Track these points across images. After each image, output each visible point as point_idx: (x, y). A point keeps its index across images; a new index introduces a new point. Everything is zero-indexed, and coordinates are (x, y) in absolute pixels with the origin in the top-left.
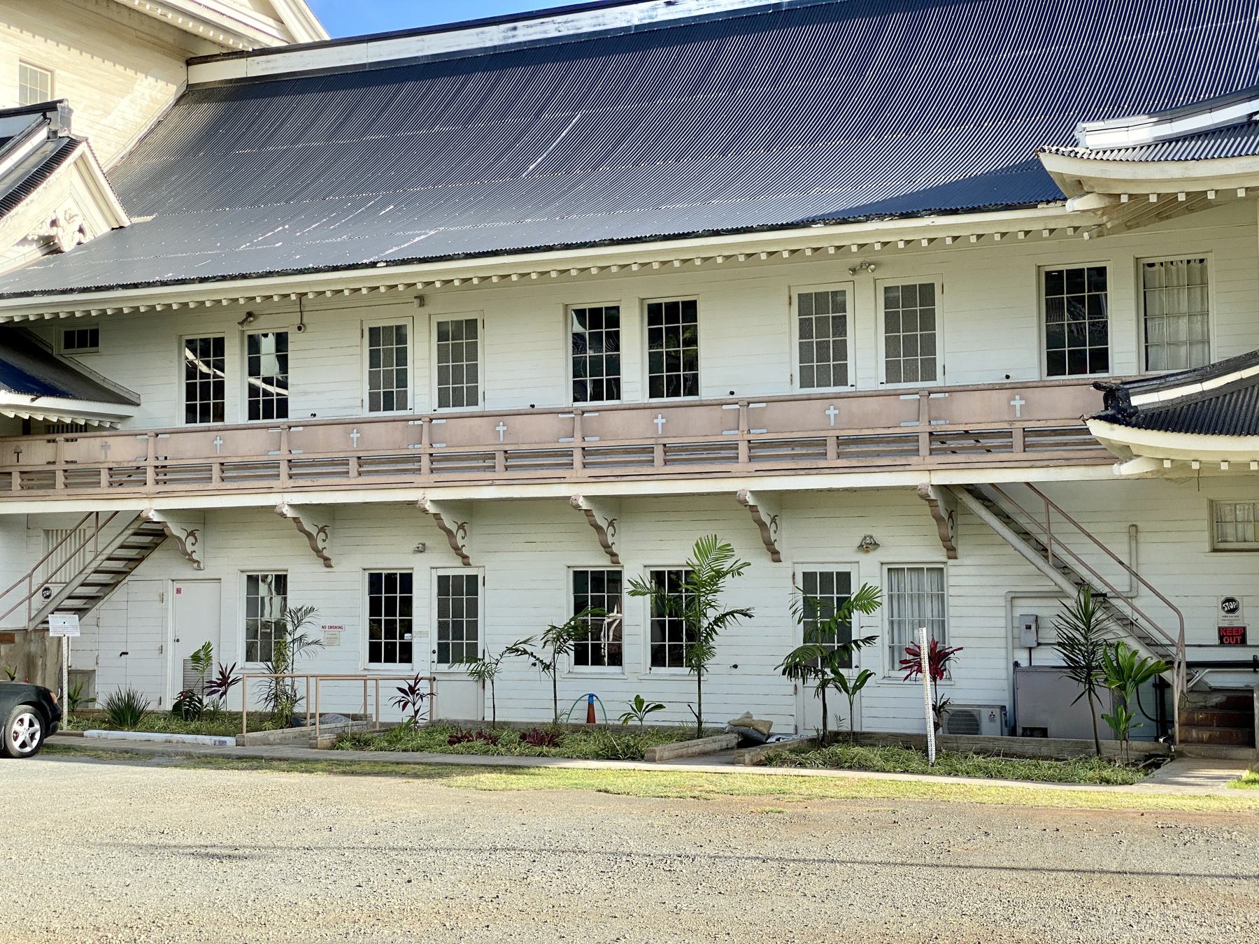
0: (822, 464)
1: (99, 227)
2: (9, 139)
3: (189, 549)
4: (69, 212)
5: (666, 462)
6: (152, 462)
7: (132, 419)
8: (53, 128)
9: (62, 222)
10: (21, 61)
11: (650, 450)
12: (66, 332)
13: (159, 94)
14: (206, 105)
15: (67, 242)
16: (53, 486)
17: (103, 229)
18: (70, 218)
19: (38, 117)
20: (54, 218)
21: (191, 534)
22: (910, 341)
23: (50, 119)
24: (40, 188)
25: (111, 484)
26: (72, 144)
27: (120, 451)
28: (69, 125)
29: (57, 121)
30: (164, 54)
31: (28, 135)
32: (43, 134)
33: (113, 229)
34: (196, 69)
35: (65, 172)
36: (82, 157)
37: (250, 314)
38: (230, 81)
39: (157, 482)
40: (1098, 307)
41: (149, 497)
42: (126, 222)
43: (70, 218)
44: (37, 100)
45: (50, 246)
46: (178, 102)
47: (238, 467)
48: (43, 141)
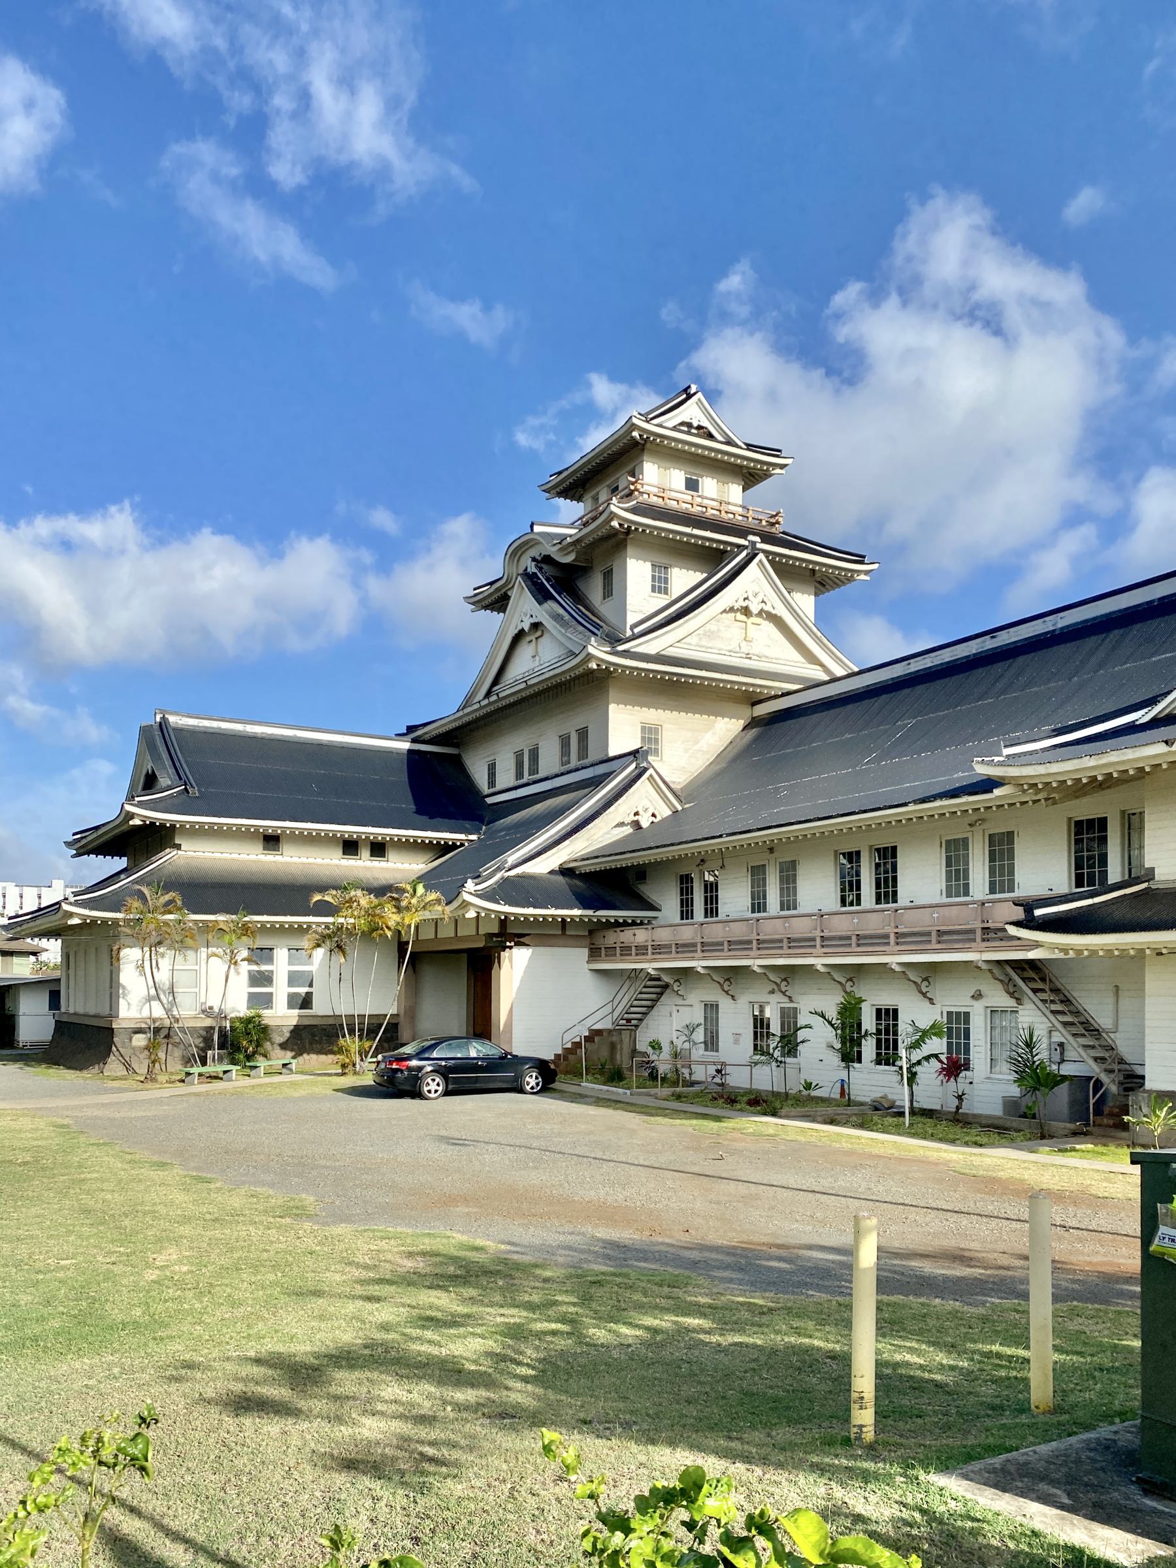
0: (929, 947)
1: (664, 812)
3: (676, 988)
5: (859, 945)
6: (650, 943)
11: (849, 938)
15: (645, 824)
16: (615, 955)
17: (670, 813)
19: (631, 758)
21: (677, 980)
22: (1002, 867)
24: (624, 798)
25: (637, 955)
26: (645, 769)
27: (641, 936)
32: (633, 766)
35: (643, 784)
36: (651, 776)
37: (702, 861)
39: (653, 954)
40: (1103, 840)
41: (650, 961)
42: (680, 808)
45: (637, 825)
46: (744, 729)
47: (684, 945)
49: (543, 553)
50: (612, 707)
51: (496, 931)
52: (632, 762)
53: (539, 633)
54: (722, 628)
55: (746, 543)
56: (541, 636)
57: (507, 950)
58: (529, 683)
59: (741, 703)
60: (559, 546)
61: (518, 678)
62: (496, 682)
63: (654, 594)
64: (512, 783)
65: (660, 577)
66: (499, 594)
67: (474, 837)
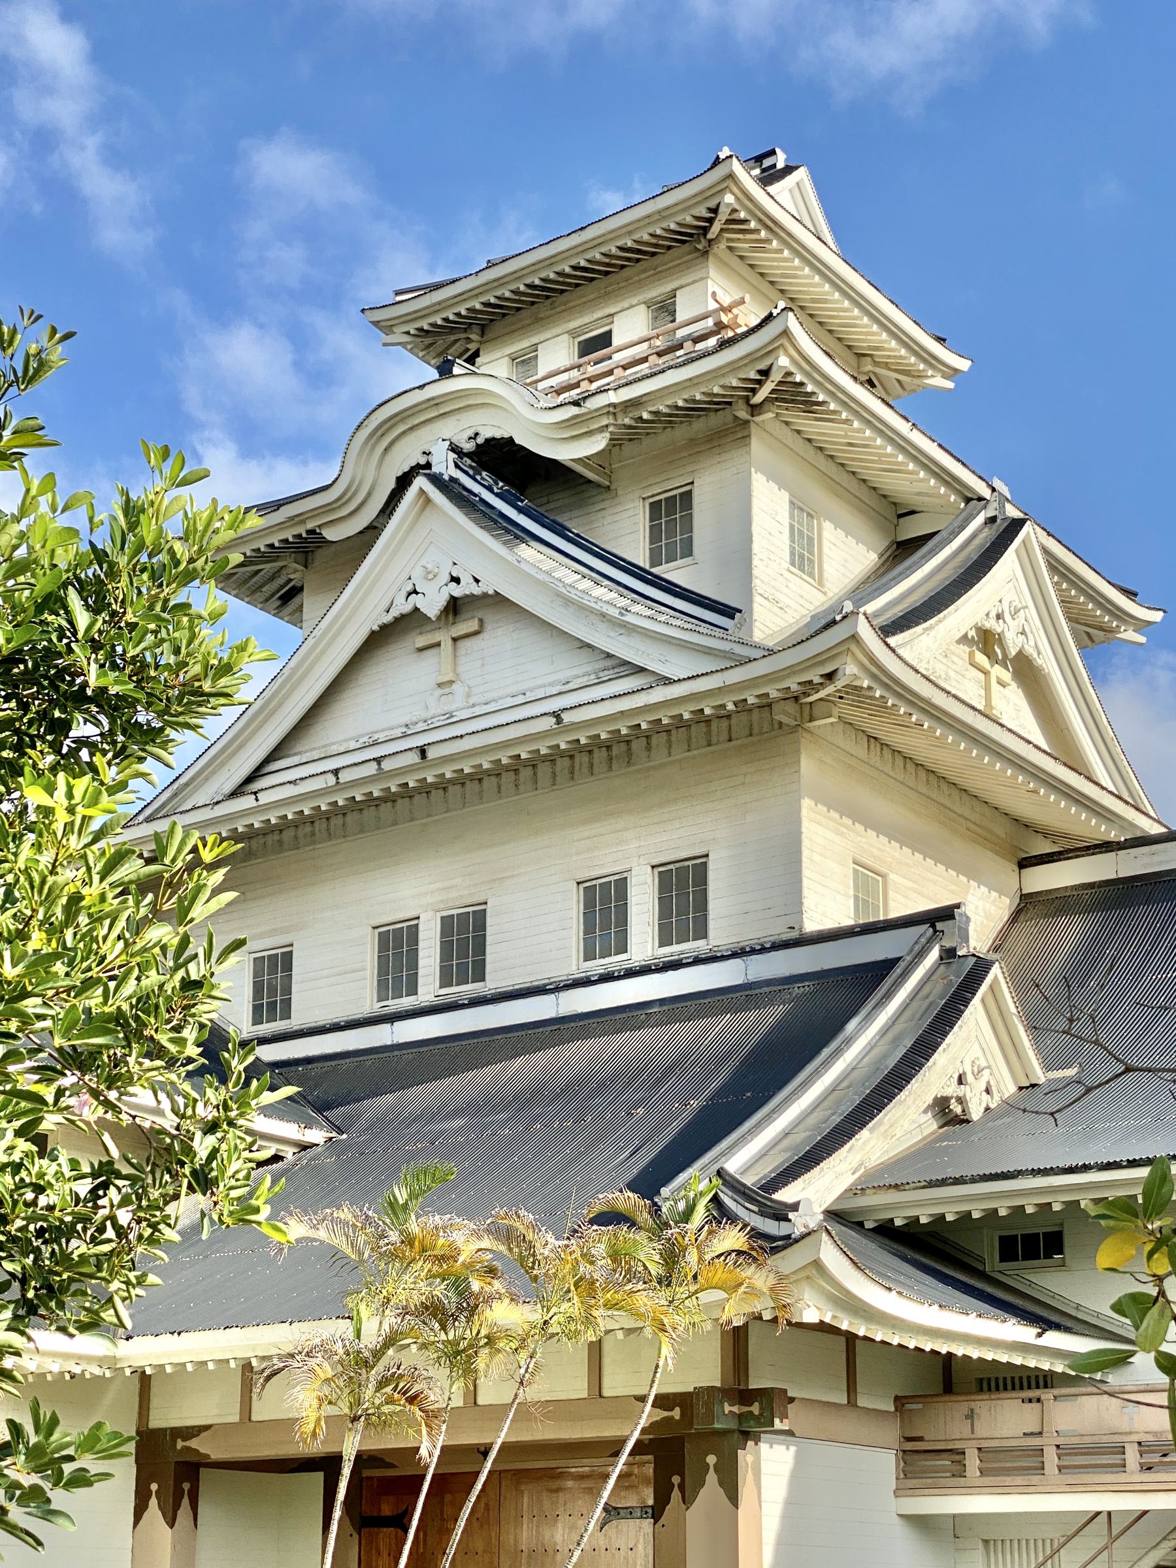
2: (899, 959)
4: (977, 1061)
7: (1132, 1365)
8: (948, 944)
9: (970, 1078)
10: (854, 863)
12: (1001, 1238)
13: (993, 908)
14: (1064, 920)
17: (1010, 1089)
18: (979, 1072)
20: (961, 1072)
23: (943, 931)
28: (967, 941)
29: (953, 934)
30: (997, 853)
31: (921, 954)
32: (934, 954)
33: (1021, 1088)
34: (1030, 872)
38: (1091, 885)
42: (1040, 1076)
43: (979, 1072)
44: (879, 916)
48: (935, 962)
49: (487, 433)
50: (806, 804)
51: (718, 1384)
52: (930, 942)
53: (473, 626)
54: (952, 674)
55: (986, 493)
56: (476, 633)
57: (750, 1443)
58: (567, 718)
59: (1003, 856)
60: (575, 410)
61: (381, 737)
62: (274, 755)
63: (792, 569)
64: (369, 1005)
65: (801, 532)
66: (289, 535)
67: (317, 1136)
